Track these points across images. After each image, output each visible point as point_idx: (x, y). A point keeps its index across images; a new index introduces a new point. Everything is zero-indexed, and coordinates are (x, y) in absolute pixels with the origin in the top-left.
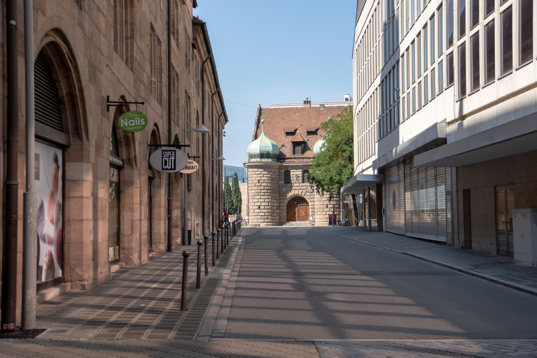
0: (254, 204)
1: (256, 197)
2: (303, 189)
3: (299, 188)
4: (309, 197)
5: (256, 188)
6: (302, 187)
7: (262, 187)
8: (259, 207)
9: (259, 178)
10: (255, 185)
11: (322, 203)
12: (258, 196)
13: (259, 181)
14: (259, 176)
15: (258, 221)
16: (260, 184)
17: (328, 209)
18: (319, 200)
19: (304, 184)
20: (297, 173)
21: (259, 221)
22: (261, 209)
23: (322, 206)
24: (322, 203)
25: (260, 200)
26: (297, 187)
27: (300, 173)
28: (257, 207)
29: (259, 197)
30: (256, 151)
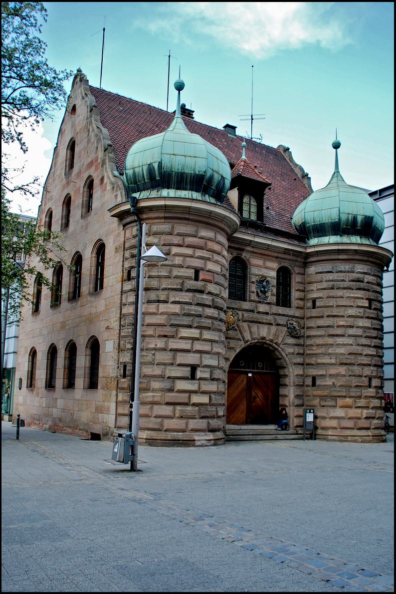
0: (174, 358)
1: (184, 332)
2: (278, 325)
3: (270, 318)
4: (291, 350)
5: (186, 297)
6: (276, 317)
7: (205, 296)
8: (194, 368)
9: (198, 263)
10: (182, 284)
11: (357, 370)
12: (190, 327)
13: (197, 272)
14: (199, 253)
15: (187, 424)
16: (199, 284)
17: (371, 392)
18: (348, 361)
19: (281, 310)
20: (265, 272)
21: (193, 424)
22: (201, 379)
23: (355, 381)
24: (357, 370)
25: (198, 346)
26: (265, 317)
27: (274, 274)
28: (186, 372)
29: (195, 333)
30: (190, 162)
